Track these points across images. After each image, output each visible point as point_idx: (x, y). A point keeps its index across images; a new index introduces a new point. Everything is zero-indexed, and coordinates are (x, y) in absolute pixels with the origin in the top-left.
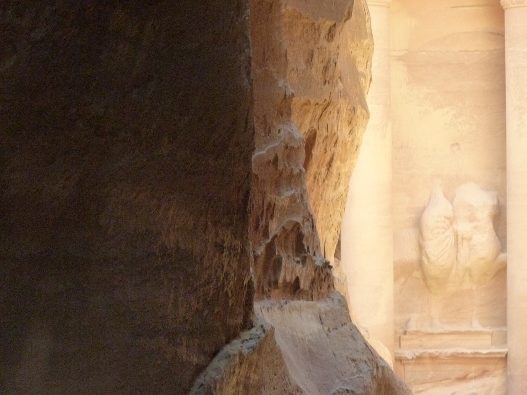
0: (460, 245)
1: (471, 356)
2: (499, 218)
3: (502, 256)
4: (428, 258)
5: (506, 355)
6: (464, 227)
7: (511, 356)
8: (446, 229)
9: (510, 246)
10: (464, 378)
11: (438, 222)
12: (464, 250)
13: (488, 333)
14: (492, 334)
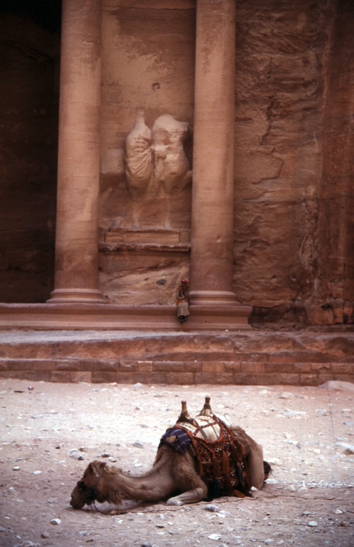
0: (156, 163)
1: (161, 249)
2: (188, 142)
3: (189, 173)
4: (130, 171)
5: (190, 250)
6: (159, 148)
7: (194, 250)
8: (145, 149)
9: (195, 163)
10: (155, 268)
11: (138, 142)
12: (159, 167)
13: (176, 233)
14: (180, 234)
